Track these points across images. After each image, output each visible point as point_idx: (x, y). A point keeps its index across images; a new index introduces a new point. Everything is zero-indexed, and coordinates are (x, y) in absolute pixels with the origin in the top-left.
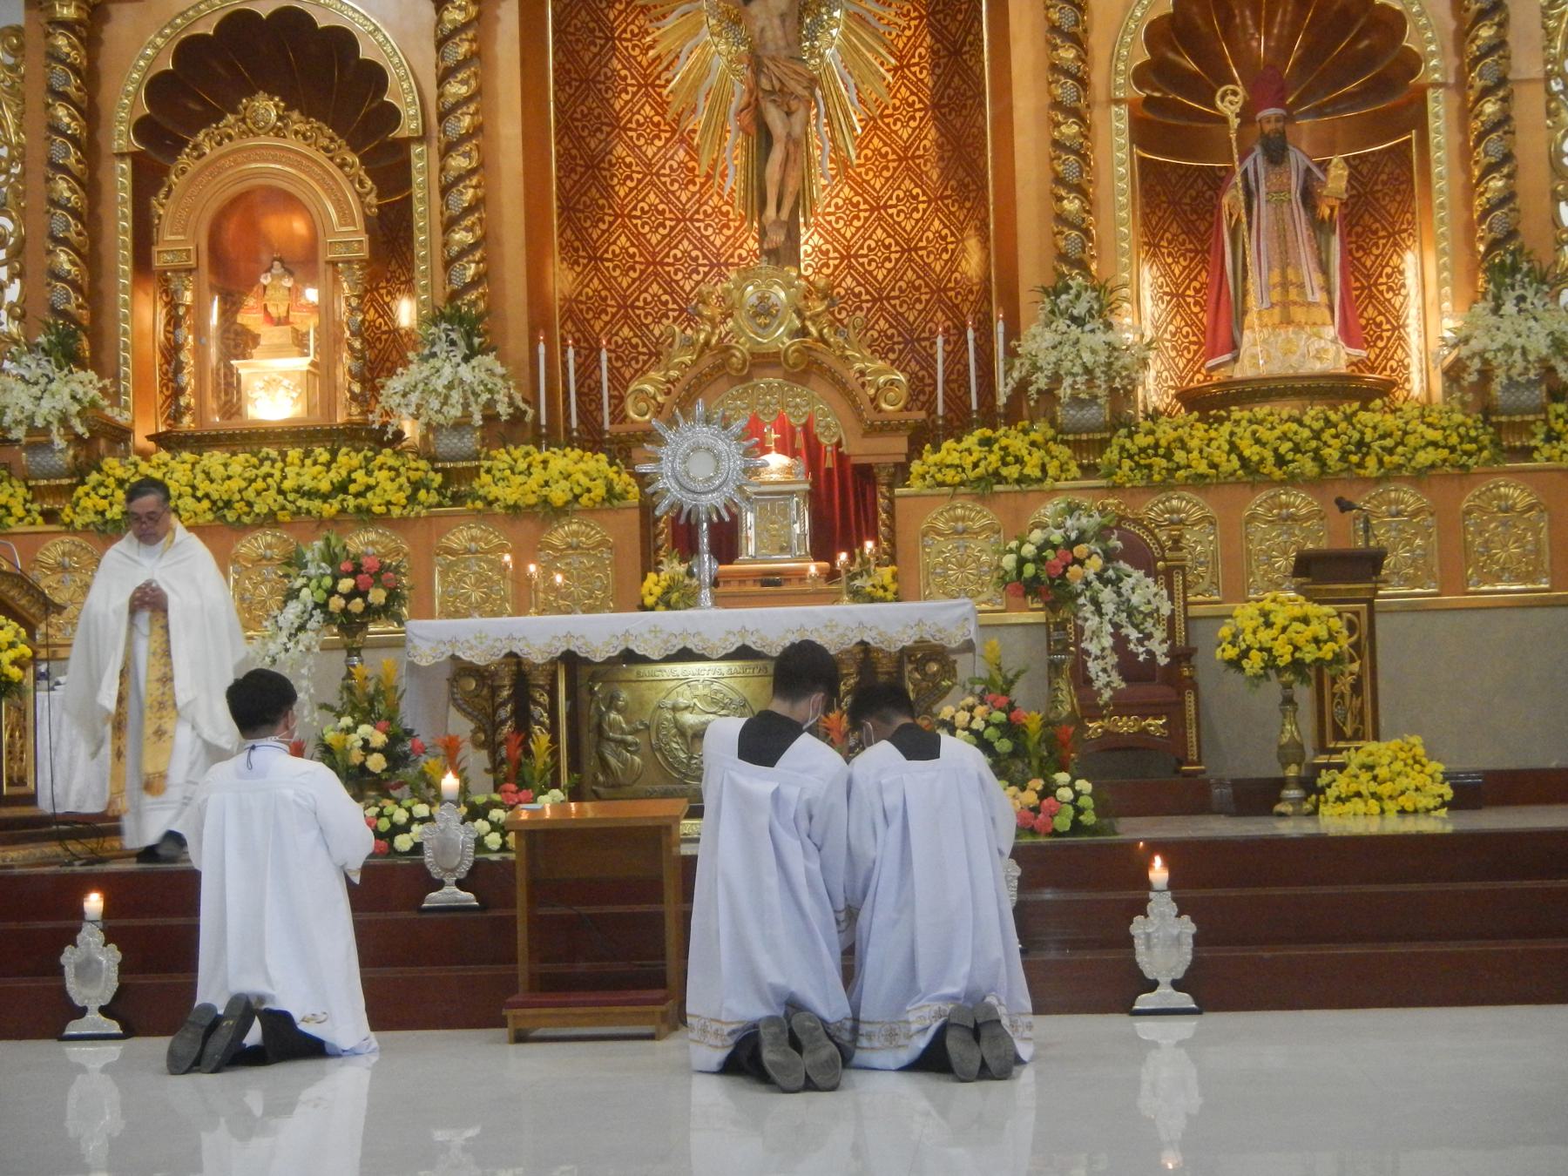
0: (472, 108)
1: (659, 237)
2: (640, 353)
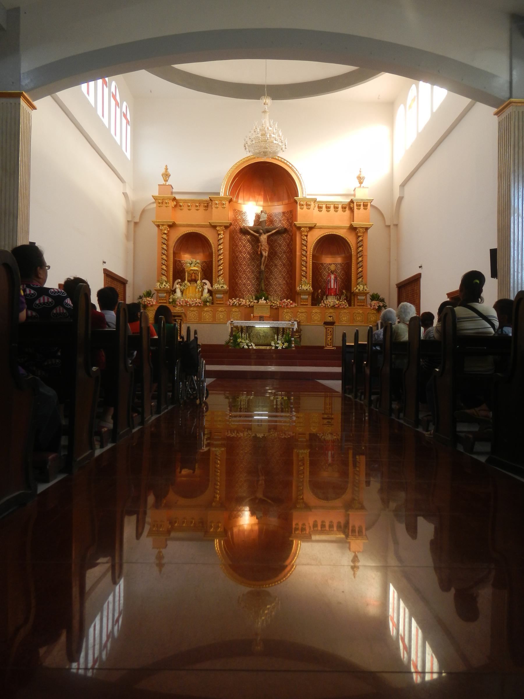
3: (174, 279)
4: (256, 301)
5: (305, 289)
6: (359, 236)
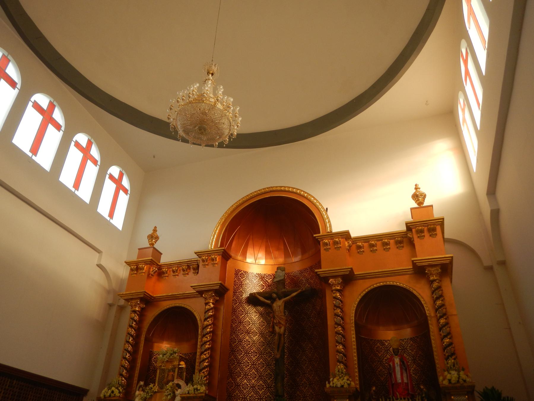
0: (210, 327)
1: (255, 358)
2: (248, 387)
5: (339, 386)
6: (432, 282)
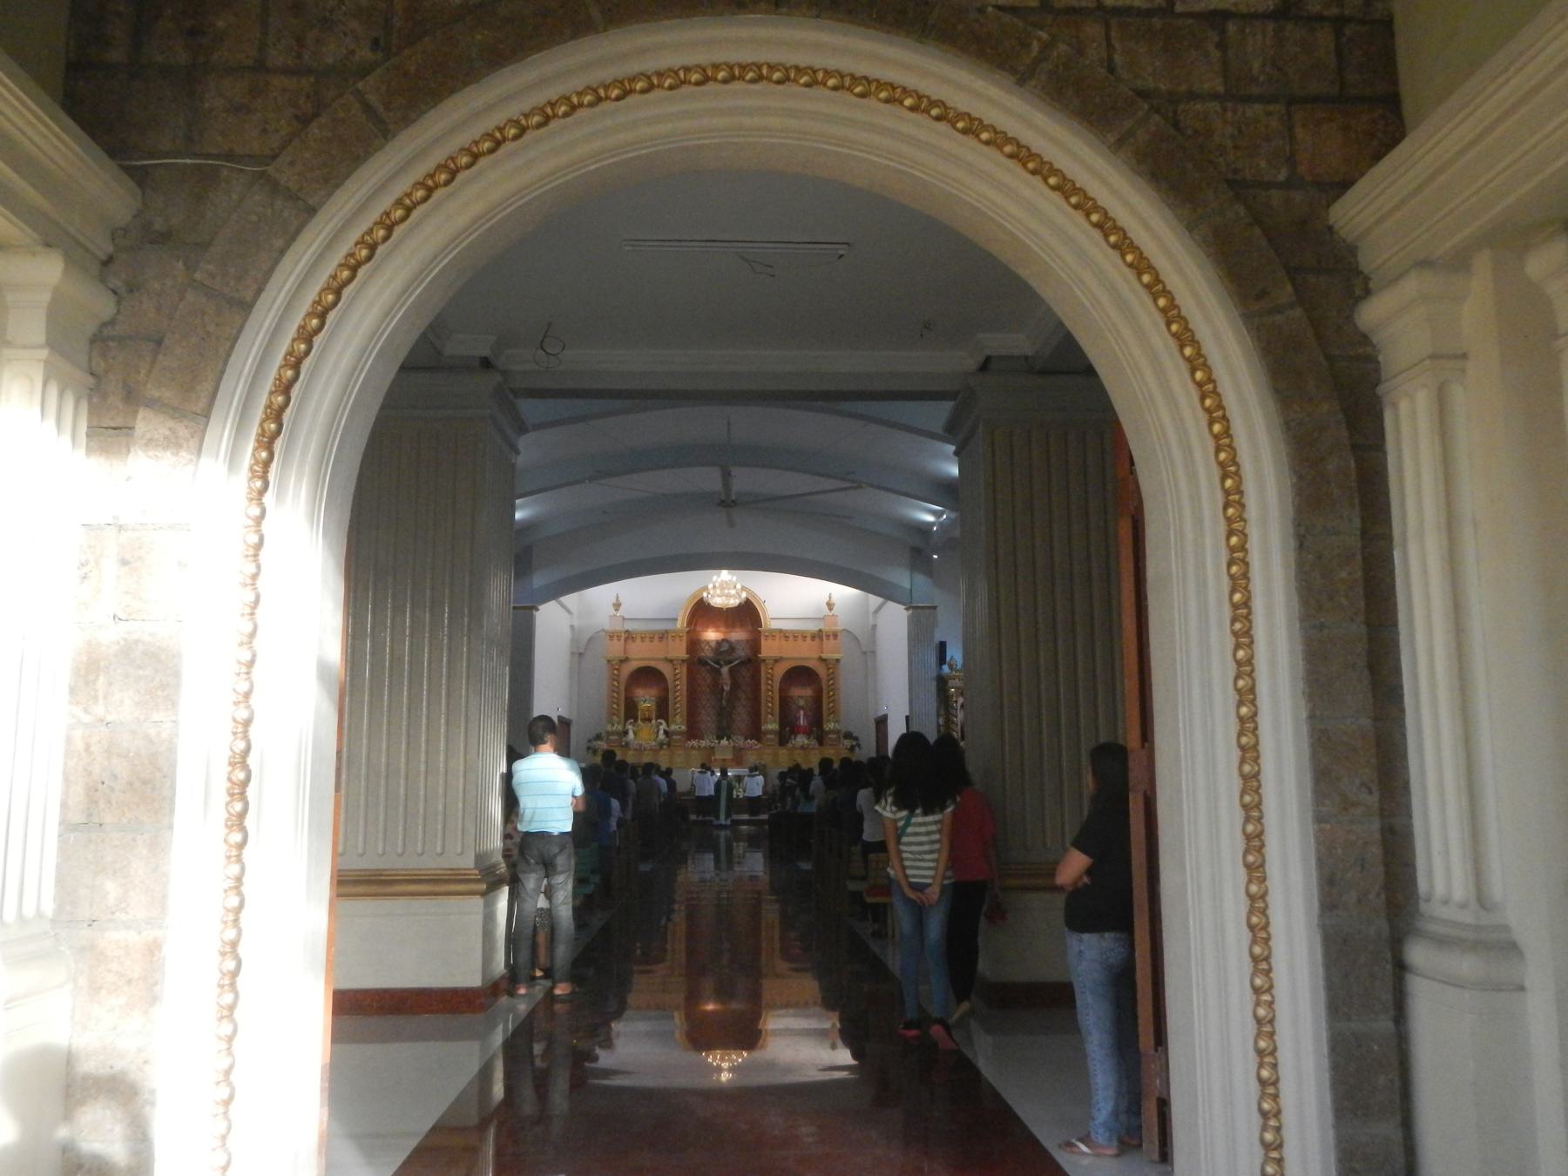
3: (627, 718)
4: (717, 741)
6: (829, 669)
